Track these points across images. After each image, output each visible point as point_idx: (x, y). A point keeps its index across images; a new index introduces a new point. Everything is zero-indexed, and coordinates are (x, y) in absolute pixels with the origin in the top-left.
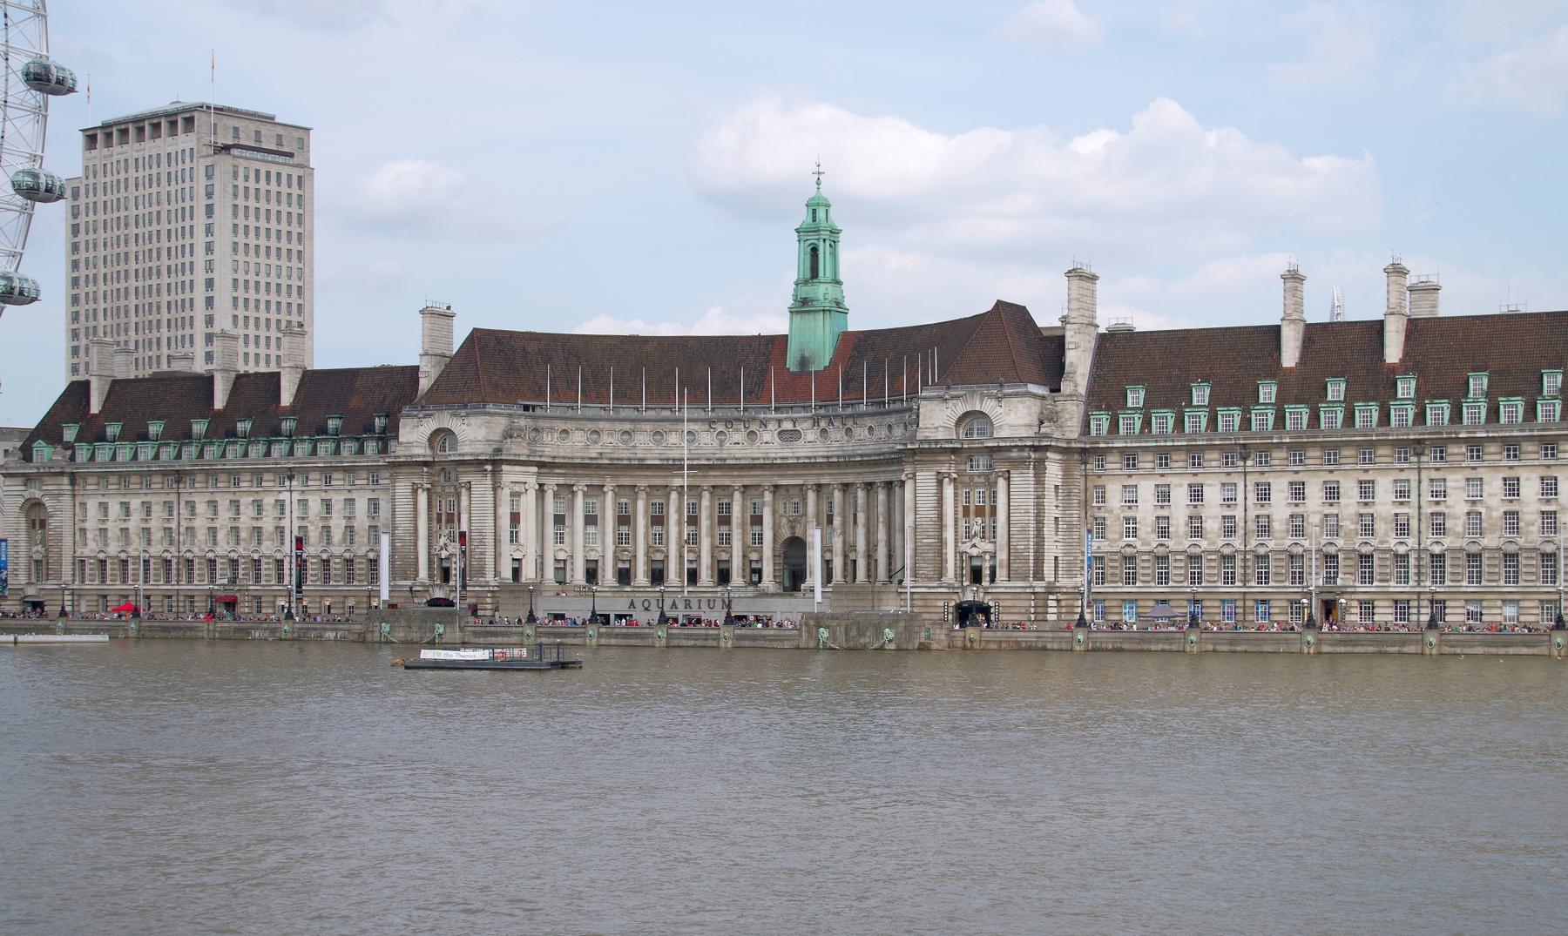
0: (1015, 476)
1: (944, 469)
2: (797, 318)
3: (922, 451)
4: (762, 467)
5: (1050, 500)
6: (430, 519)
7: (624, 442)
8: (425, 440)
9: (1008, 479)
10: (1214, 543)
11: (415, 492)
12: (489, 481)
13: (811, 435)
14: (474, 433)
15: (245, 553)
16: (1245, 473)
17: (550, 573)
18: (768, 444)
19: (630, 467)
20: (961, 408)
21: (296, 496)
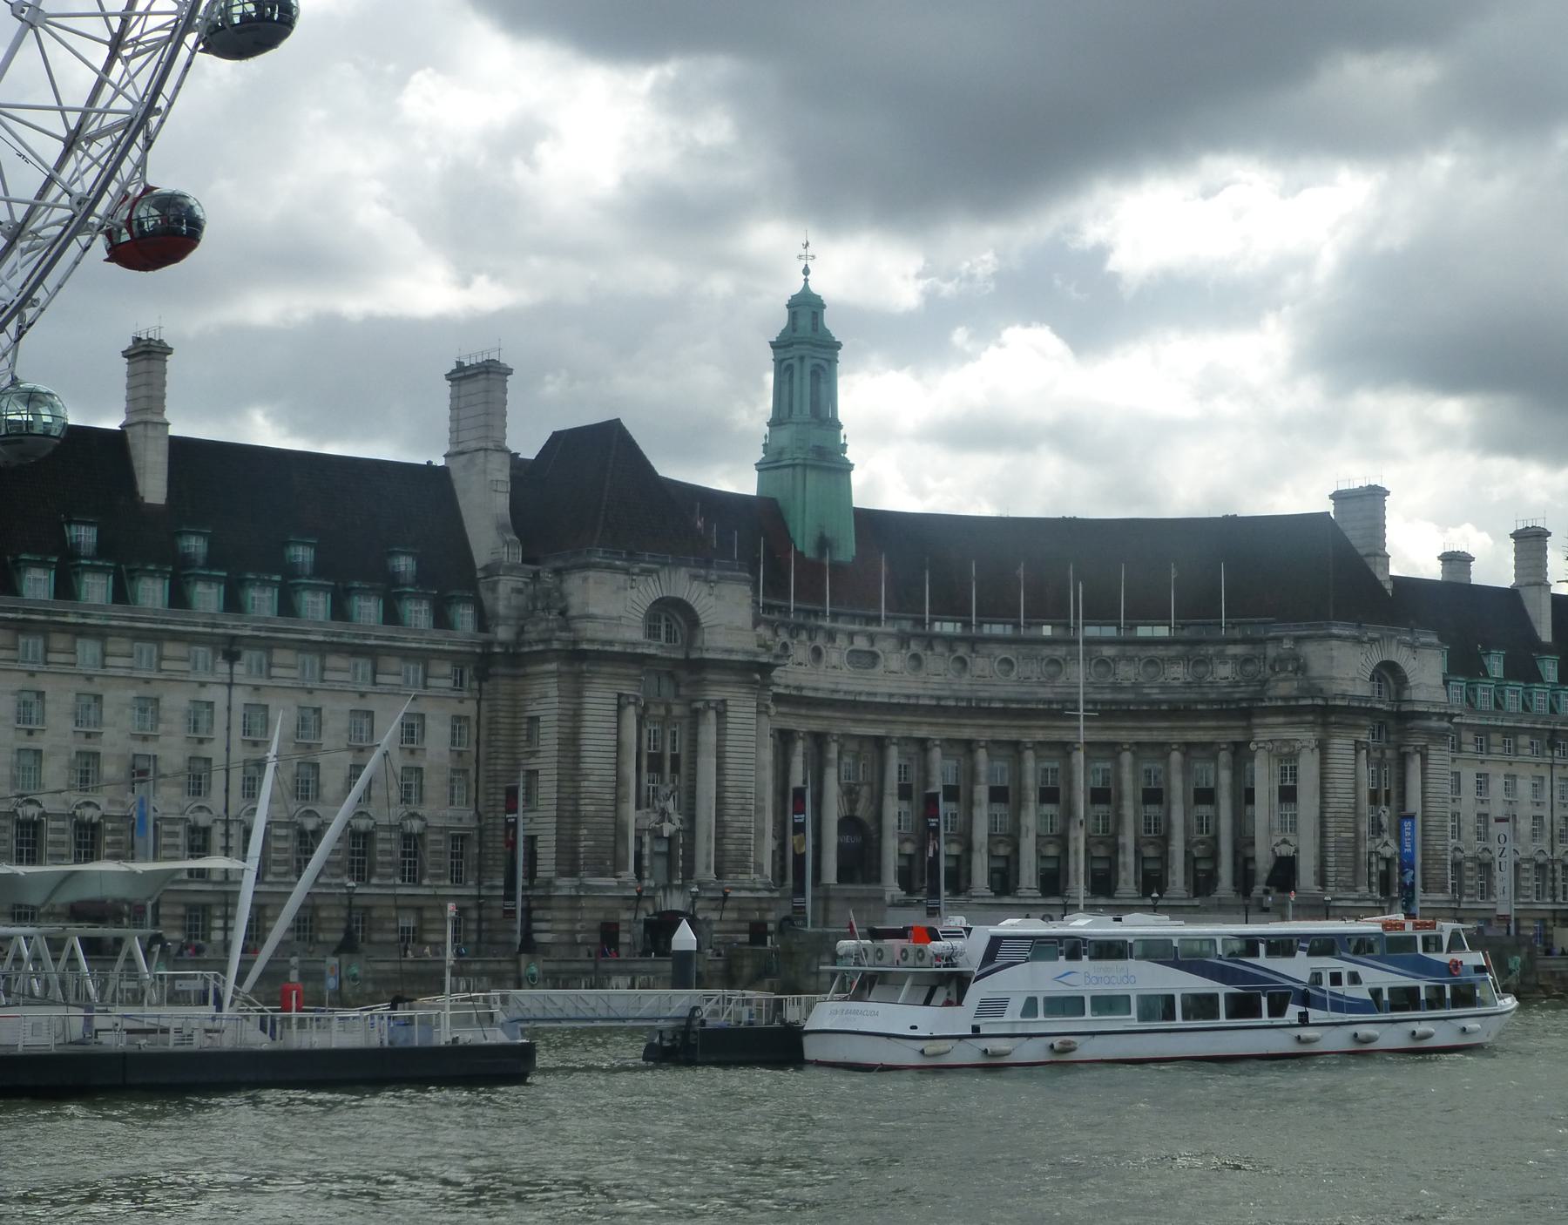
2: (812, 477)
9: (1424, 759)
11: (620, 709)
13: (894, 660)
15: (116, 811)
16: (1552, 766)
20: (1376, 657)
21: (241, 697)
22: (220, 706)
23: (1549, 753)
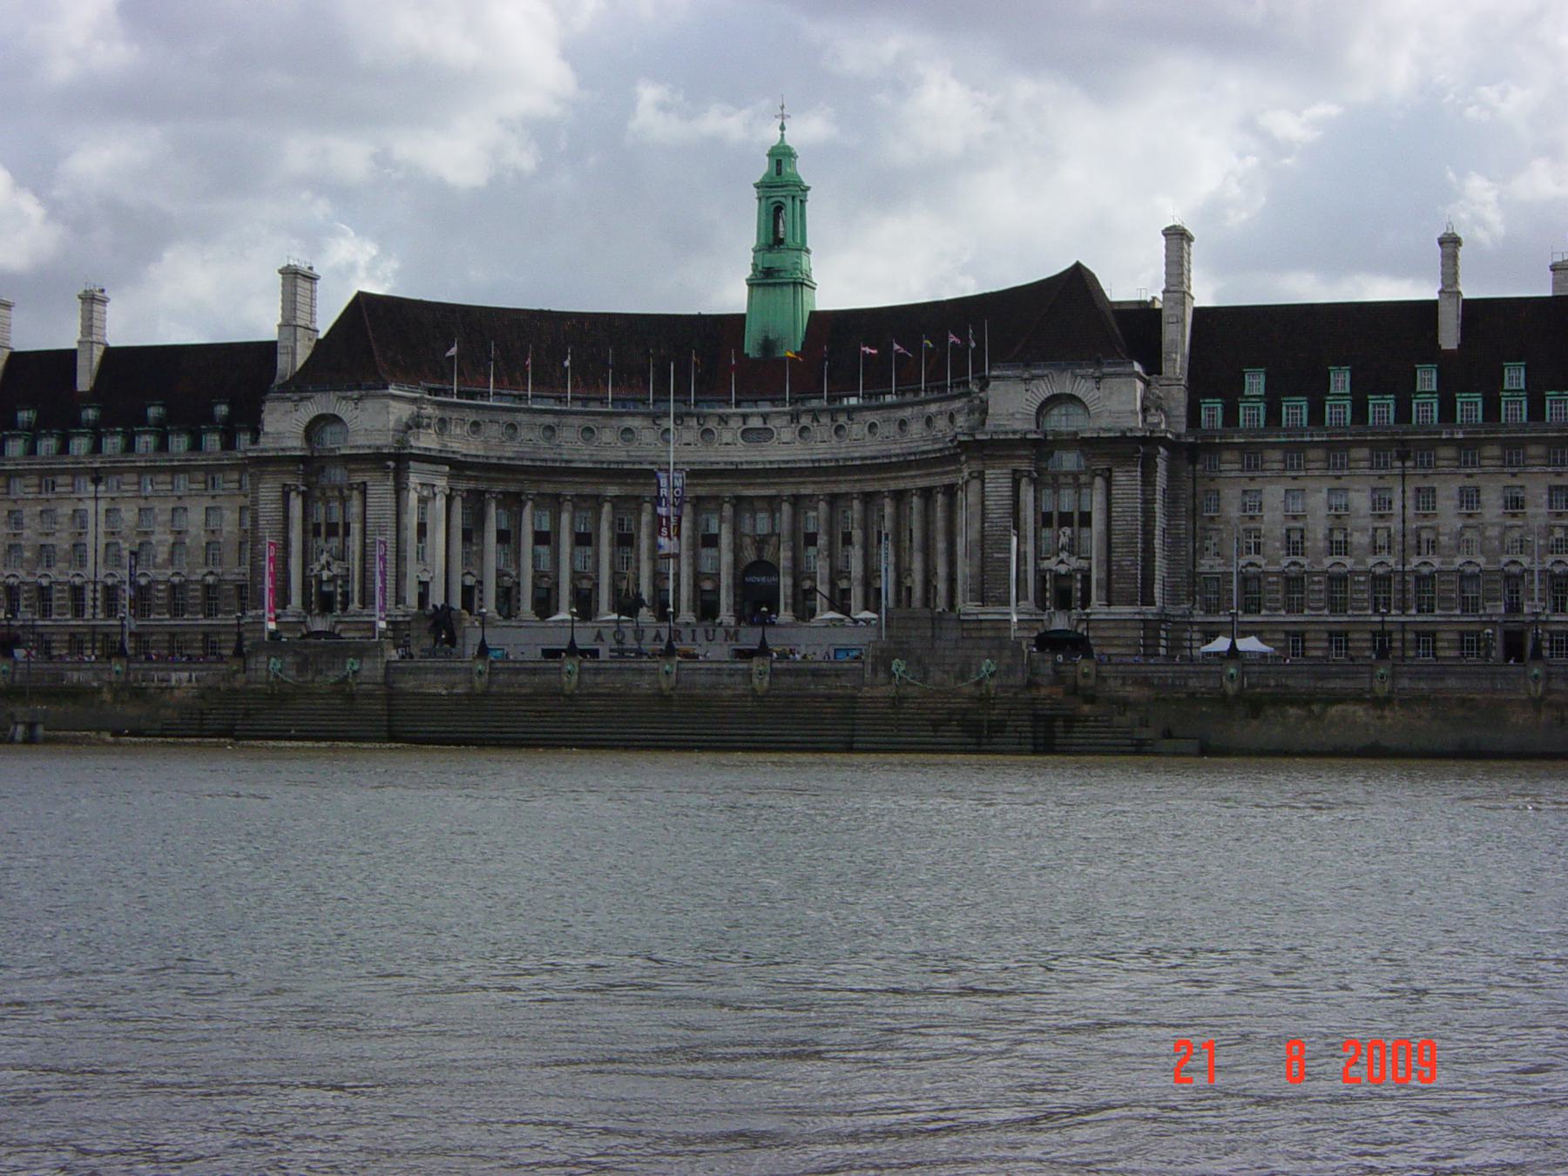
0: (1120, 477)
1: (1024, 466)
2: (759, 292)
3: (992, 443)
4: (721, 473)
5: (1158, 507)
6: (305, 531)
7: (548, 439)
8: (301, 430)
10: (1363, 562)
12: (391, 483)
13: (786, 435)
14: (373, 420)
16: (1404, 476)
17: (457, 603)
18: (729, 447)
19: (554, 471)
20: (1044, 390)
21: (103, 505)
22: (91, 512)
23: (1399, 464)
